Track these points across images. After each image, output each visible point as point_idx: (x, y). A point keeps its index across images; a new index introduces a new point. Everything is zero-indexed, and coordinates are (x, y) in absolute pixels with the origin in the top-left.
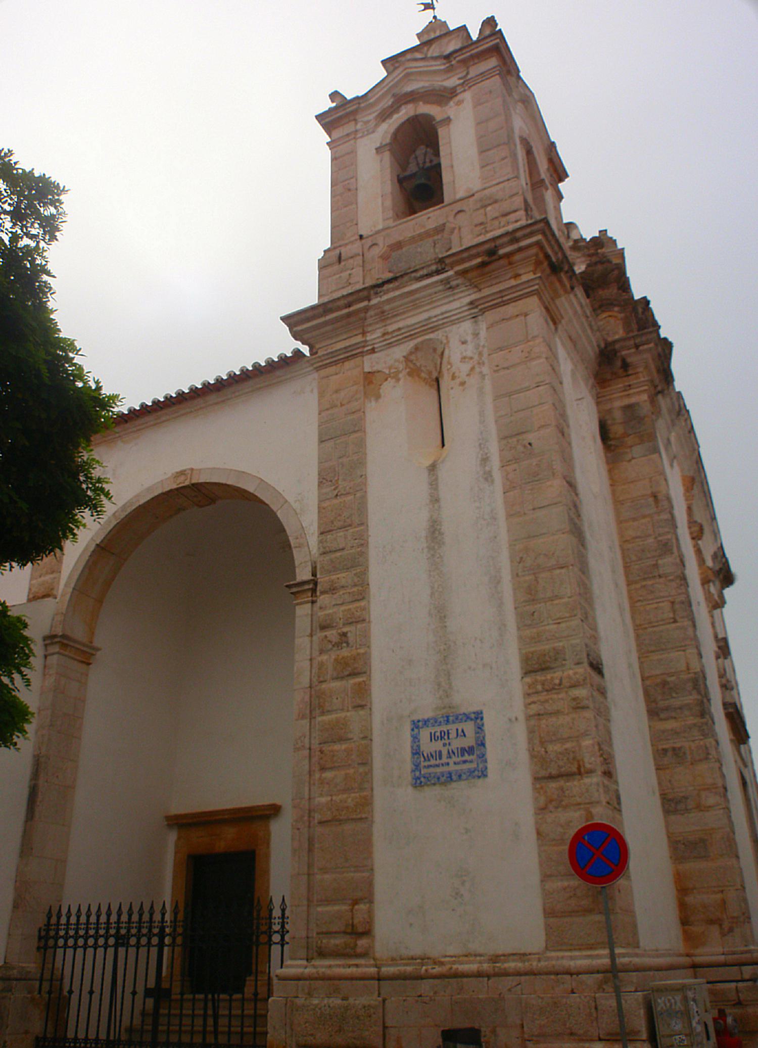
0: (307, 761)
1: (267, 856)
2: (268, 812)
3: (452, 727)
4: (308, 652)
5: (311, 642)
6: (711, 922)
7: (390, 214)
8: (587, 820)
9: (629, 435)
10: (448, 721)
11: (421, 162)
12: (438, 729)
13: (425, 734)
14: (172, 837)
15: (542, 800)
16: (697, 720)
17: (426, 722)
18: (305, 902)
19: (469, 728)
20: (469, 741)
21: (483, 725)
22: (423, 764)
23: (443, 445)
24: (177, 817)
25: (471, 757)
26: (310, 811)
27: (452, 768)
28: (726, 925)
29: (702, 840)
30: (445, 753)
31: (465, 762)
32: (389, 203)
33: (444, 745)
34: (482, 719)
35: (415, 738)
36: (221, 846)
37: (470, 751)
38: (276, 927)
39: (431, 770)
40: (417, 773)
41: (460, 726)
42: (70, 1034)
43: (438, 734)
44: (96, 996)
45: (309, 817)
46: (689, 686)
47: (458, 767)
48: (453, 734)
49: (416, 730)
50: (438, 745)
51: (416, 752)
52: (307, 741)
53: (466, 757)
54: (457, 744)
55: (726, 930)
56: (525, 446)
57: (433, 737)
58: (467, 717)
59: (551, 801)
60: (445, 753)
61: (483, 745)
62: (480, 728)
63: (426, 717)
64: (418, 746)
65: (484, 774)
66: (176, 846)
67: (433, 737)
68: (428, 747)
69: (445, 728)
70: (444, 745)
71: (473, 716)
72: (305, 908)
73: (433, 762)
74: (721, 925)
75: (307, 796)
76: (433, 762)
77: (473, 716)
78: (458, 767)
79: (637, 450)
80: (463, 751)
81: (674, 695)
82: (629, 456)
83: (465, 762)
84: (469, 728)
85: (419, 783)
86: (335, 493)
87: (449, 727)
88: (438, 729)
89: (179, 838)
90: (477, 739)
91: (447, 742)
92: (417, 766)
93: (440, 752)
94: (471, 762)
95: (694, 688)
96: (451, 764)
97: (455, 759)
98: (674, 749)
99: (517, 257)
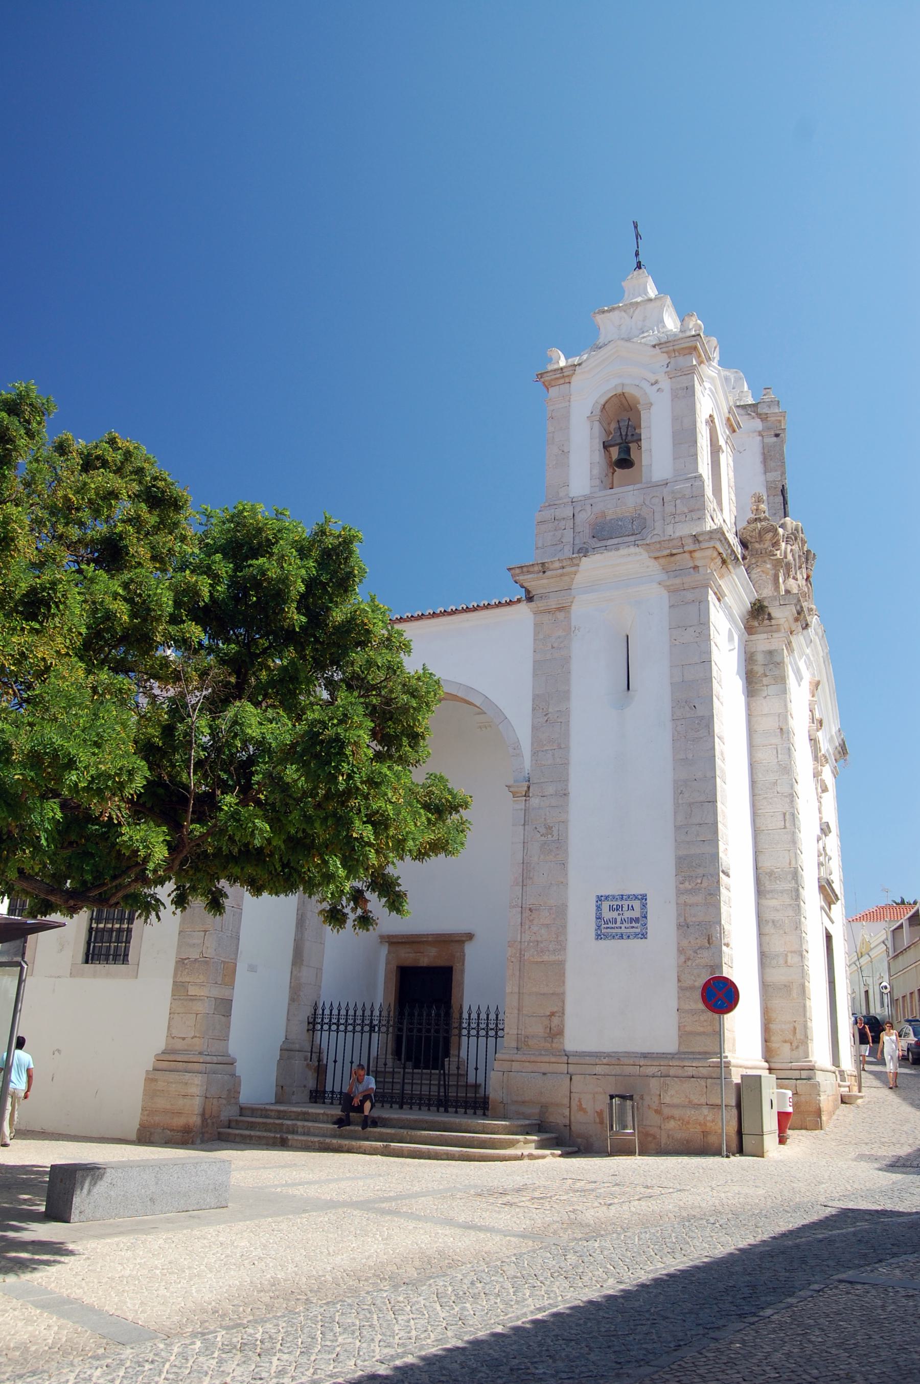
0: (520, 916)
1: (462, 971)
2: (464, 939)
3: (625, 903)
4: (522, 838)
5: (524, 830)
6: (785, 1042)
7: (597, 482)
8: (711, 974)
9: (766, 676)
10: (622, 898)
11: (624, 433)
12: (615, 903)
13: (605, 905)
14: (384, 950)
15: (683, 959)
16: (792, 902)
17: (607, 897)
18: (516, 1011)
19: (637, 904)
20: (636, 914)
21: (646, 904)
22: (603, 926)
23: (628, 688)
24: (389, 937)
25: (637, 925)
26: (521, 950)
27: (623, 930)
28: (795, 1044)
29: (785, 986)
30: (619, 920)
31: (633, 927)
32: (596, 471)
33: (619, 914)
34: (646, 900)
35: (599, 908)
36: (424, 962)
37: (637, 920)
38: (465, 1025)
39: (609, 930)
40: (599, 932)
41: (631, 903)
42: (329, 1088)
43: (615, 907)
44: (339, 1064)
45: (520, 954)
46: (789, 877)
47: (628, 930)
48: (625, 908)
49: (599, 902)
50: (614, 914)
51: (599, 917)
52: (520, 901)
53: (634, 924)
54: (628, 914)
55: (794, 1047)
56: (690, 708)
57: (611, 908)
58: (636, 897)
59: (689, 959)
60: (619, 920)
61: (646, 917)
62: (644, 906)
63: (607, 894)
64: (600, 913)
65: (644, 936)
66: (387, 959)
67: (611, 908)
68: (607, 914)
69: (620, 903)
70: (619, 914)
71: (640, 897)
72: (516, 1015)
73: (610, 925)
74: (791, 1044)
75: (519, 940)
76: (610, 925)
77: (640, 897)
78: (628, 930)
79: (772, 690)
80: (632, 919)
81: (778, 882)
82: (765, 694)
83: (633, 927)
84: (637, 904)
85: (599, 937)
86: (546, 718)
87: (623, 902)
88: (615, 903)
89: (389, 952)
90: (642, 913)
91: (621, 913)
92: (599, 927)
93: (616, 919)
94: (637, 928)
95: (793, 879)
96: (623, 928)
97: (625, 925)
98: (773, 922)
99: (697, 555)
